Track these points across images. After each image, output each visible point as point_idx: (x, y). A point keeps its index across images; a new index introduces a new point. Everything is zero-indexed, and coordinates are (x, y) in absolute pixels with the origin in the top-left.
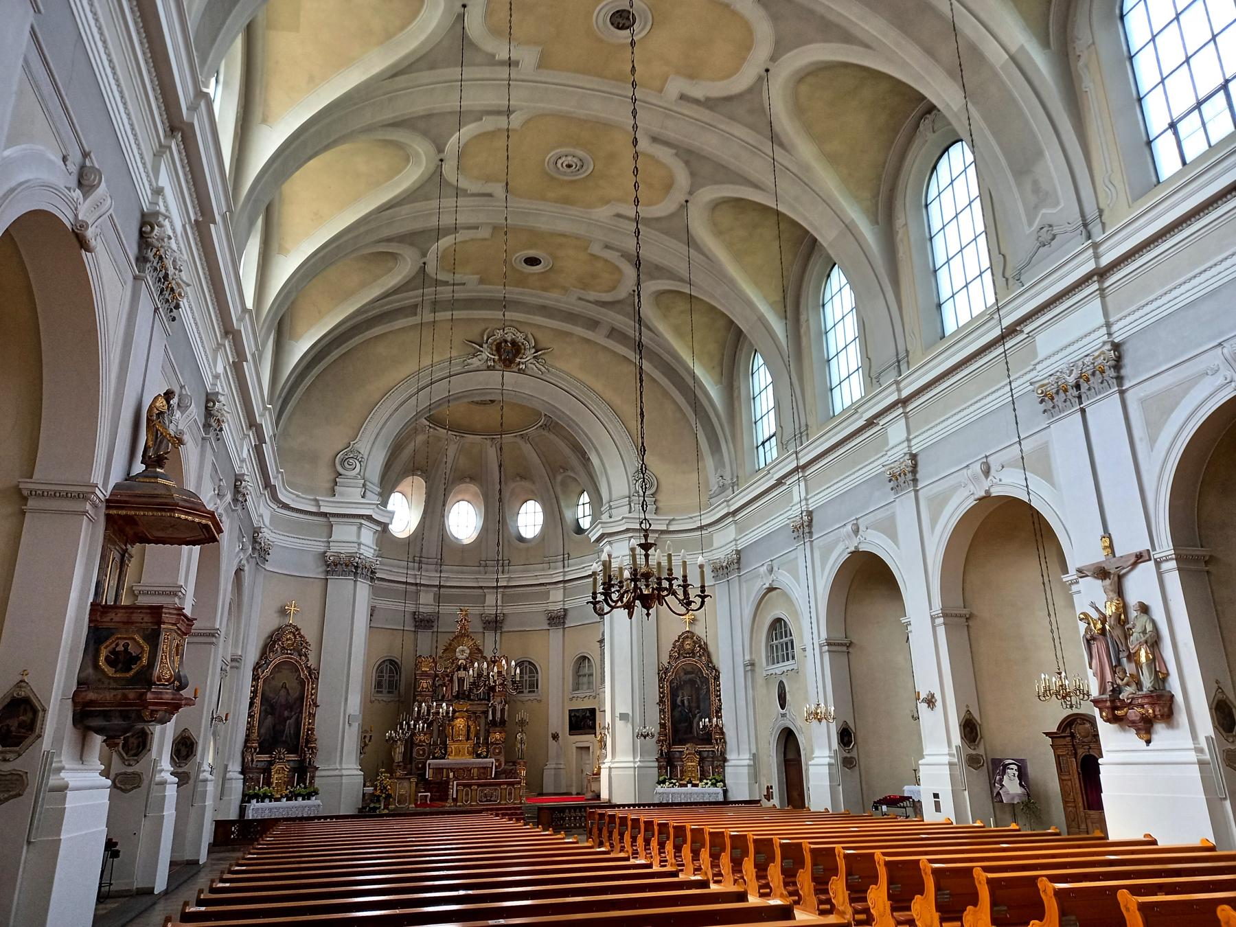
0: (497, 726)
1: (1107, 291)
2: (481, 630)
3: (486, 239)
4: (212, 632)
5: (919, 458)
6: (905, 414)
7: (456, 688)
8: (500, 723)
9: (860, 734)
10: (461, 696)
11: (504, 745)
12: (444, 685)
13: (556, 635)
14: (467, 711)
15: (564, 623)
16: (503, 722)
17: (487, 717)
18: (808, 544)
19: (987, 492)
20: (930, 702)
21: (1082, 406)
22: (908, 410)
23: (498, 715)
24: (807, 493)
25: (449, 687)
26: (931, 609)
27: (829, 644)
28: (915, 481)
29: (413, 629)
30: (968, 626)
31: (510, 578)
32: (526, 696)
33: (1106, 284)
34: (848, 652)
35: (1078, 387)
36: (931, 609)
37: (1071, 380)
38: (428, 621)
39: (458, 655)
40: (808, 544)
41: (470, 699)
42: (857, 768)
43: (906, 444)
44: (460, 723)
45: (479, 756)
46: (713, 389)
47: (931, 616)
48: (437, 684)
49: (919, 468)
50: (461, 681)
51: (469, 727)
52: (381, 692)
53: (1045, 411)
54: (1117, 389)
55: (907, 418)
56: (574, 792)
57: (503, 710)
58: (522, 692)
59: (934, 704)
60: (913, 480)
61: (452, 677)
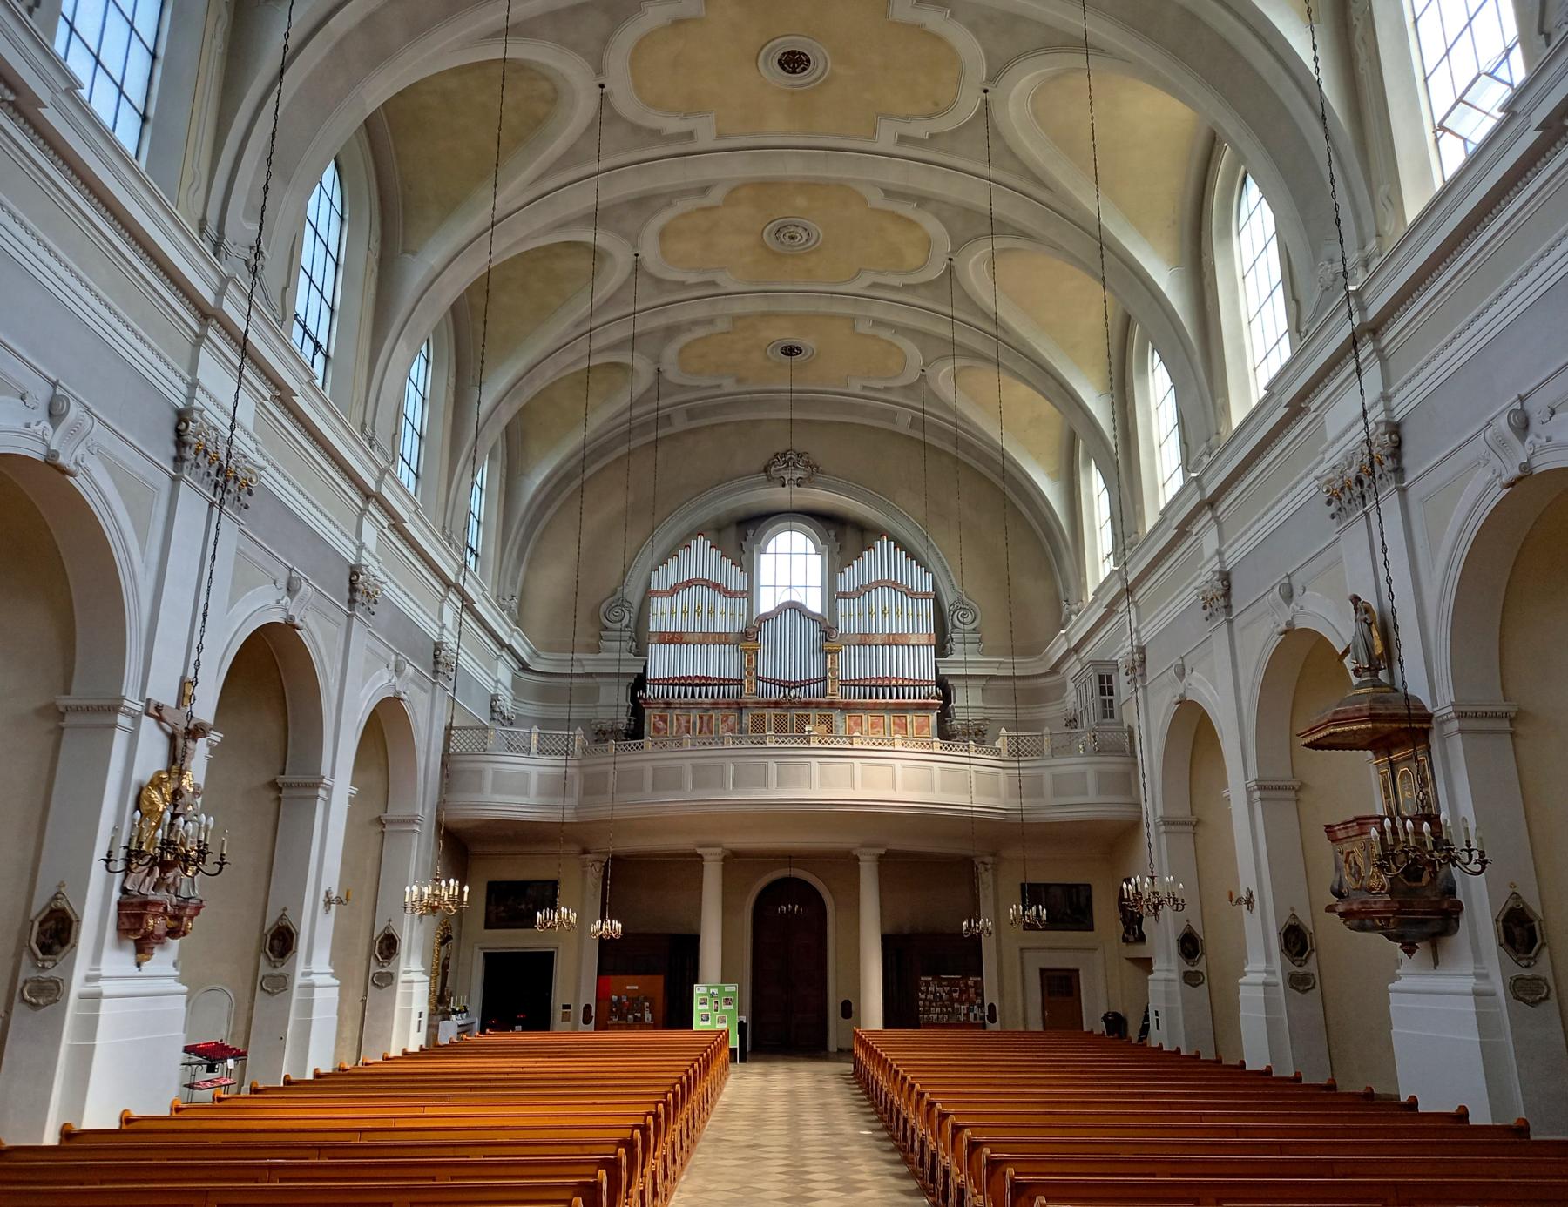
1: (1386, 352)
3: (728, 333)
4: (413, 818)
5: (1234, 578)
6: (1216, 519)
9: (1210, 944)
18: (1140, 691)
19: (1289, 623)
20: (1249, 902)
21: (1365, 509)
22: (1219, 513)
24: (1139, 623)
26: (1247, 779)
27: (1165, 823)
28: (1228, 607)
30: (1297, 800)
33: (1385, 342)
34: (1194, 834)
35: (1360, 482)
36: (1246, 779)
37: (1352, 473)
40: (1140, 691)
42: (1205, 986)
43: (1216, 559)
46: (1049, 488)
47: (1247, 789)
49: (1234, 591)
53: (1333, 516)
54: (1393, 486)
55: (1219, 524)
59: (1252, 907)
60: (1225, 607)
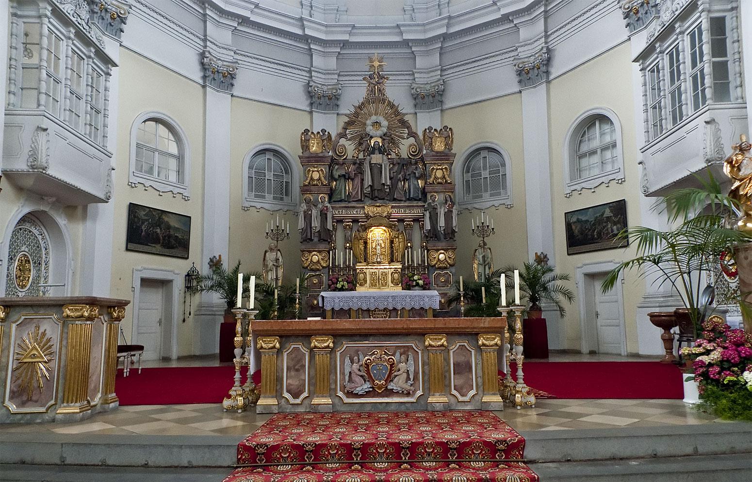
0: (439, 239)
2: (413, 111)
7: (368, 181)
8: (445, 234)
10: (376, 195)
11: (453, 270)
12: (346, 177)
13: (533, 99)
14: (389, 217)
15: (547, 73)
16: (450, 234)
17: (422, 227)
23: (442, 222)
25: (357, 181)
29: (308, 109)
31: (450, 18)
32: (487, 200)
38: (330, 99)
39: (370, 129)
41: (395, 200)
44: (378, 235)
45: (408, 287)
48: (336, 174)
50: (376, 170)
51: (392, 242)
52: (264, 197)
56: (585, 349)
57: (448, 216)
58: (481, 197)
61: (361, 164)
